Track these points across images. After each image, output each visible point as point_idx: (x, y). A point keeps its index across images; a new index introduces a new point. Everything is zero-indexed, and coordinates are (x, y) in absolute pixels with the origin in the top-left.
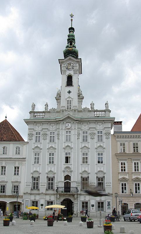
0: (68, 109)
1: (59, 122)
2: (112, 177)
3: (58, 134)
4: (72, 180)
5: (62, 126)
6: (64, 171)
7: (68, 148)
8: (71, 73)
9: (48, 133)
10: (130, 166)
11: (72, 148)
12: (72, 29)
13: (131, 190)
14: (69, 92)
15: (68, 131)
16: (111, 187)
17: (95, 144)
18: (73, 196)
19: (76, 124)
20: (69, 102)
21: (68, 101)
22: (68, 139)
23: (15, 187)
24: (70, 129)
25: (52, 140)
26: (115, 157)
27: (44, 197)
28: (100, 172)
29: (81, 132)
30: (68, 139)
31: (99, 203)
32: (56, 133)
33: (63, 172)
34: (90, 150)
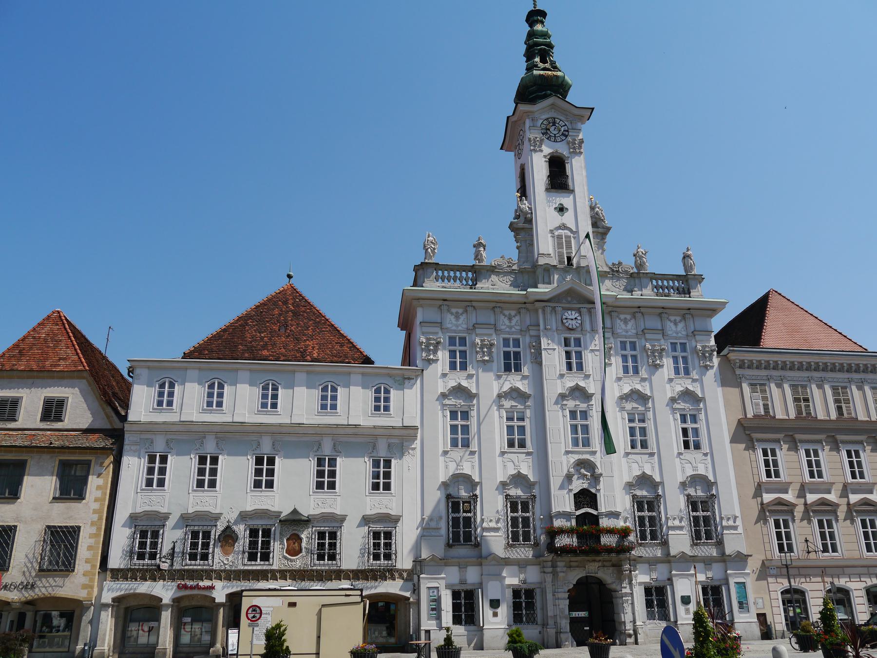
1: (538, 304)
7: (577, 394)
8: (562, 149)
13: (806, 541)
16: (740, 530)
18: (613, 566)
22: (575, 362)
30: (575, 362)
32: (525, 340)
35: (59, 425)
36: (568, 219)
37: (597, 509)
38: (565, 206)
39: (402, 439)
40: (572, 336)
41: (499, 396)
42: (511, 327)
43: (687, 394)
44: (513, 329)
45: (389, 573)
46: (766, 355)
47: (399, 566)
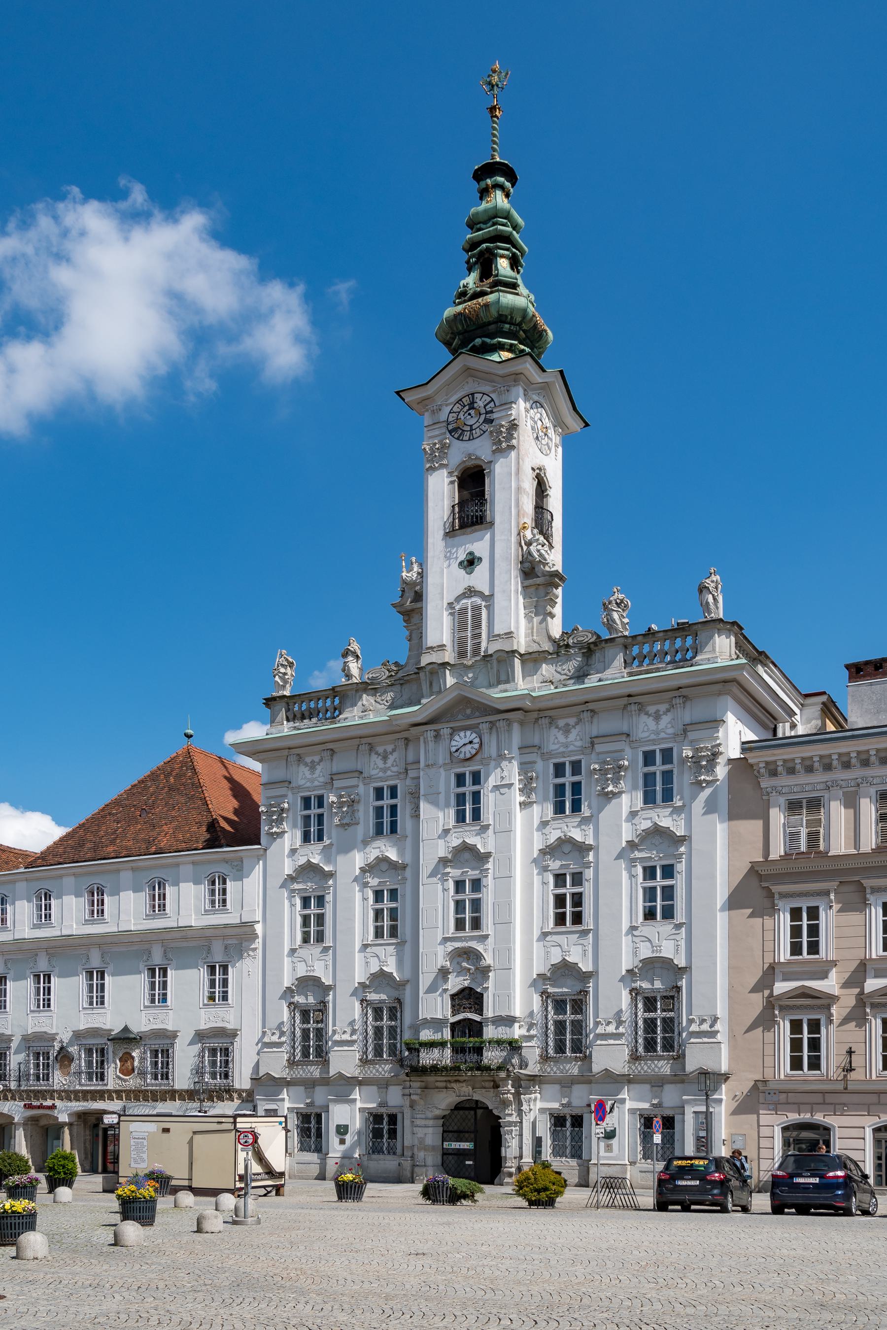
14: (471, 562)
19: (509, 731)
24: (478, 757)
36: (479, 578)
38: (477, 554)
39: (239, 938)
40: (467, 770)
41: (543, 852)
42: (385, 770)
43: (657, 833)
44: (389, 773)
46: (770, 752)
47: (237, 1086)
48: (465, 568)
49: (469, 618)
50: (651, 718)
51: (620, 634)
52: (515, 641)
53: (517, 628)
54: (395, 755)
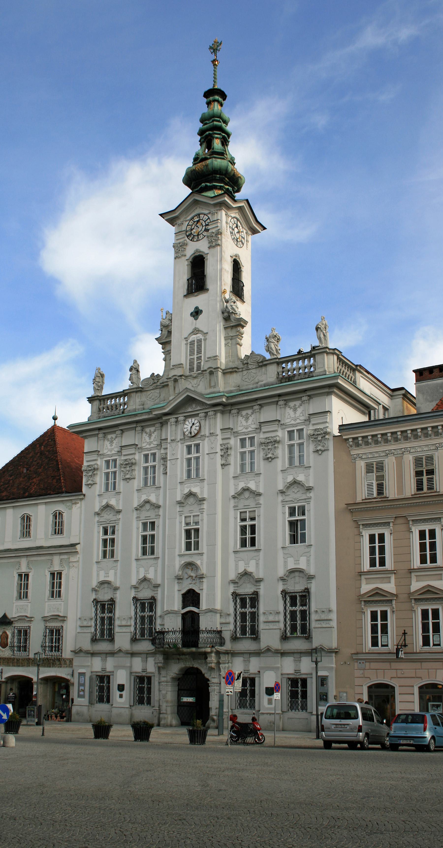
0: (191, 369)
2: (338, 589)
3: (164, 459)
4: (204, 605)
5: (170, 431)
6: (179, 579)
7: (191, 500)
9: (139, 457)
10: (403, 545)
11: (203, 499)
12: (214, 94)
13: (405, 633)
14: (197, 313)
15: (193, 441)
16: (334, 624)
17: (280, 477)
19: (215, 418)
20: (196, 347)
21: (192, 343)
23: (51, 632)
24: (199, 436)
25: (150, 481)
26: (348, 517)
27: (126, 661)
28: (297, 574)
29: (234, 442)
31: (294, 682)
33: (176, 581)
34: (261, 500)
35: (383, 496)
37: (199, 608)
42: (150, 443)
45: (57, 662)
48: (194, 317)
49: (196, 347)
50: (292, 410)
51: (275, 357)
52: (219, 362)
53: (220, 353)
54: (156, 433)
